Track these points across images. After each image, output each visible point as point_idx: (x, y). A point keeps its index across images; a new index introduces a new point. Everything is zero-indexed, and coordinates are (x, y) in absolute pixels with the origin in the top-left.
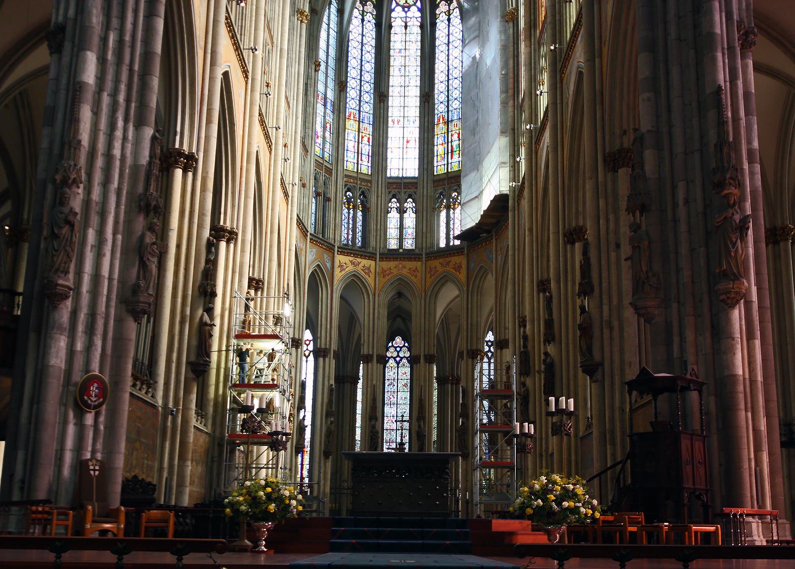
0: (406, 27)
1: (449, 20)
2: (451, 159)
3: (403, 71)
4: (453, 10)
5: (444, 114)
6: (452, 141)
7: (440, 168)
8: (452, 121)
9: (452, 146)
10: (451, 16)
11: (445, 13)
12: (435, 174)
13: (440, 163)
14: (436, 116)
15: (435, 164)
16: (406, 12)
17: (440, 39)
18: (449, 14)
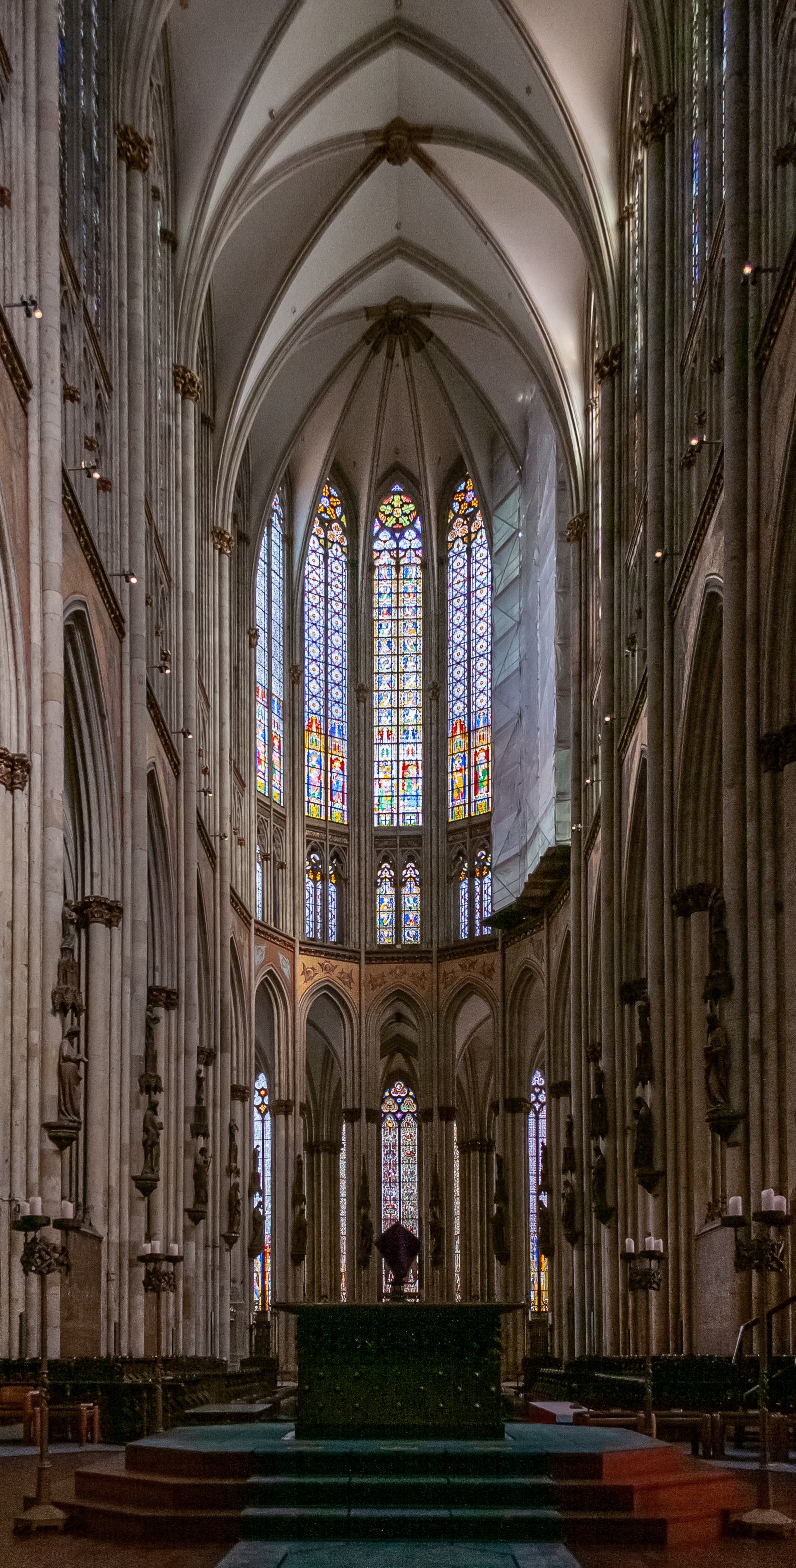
0: (398, 567)
1: (469, 551)
2: (476, 794)
3: (394, 647)
4: (477, 533)
5: (462, 719)
6: (476, 764)
7: (457, 812)
8: (476, 730)
9: (477, 774)
10: (474, 545)
11: (463, 538)
12: (451, 820)
13: (458, 803)
14: (450, 723)
15: (451, 805)
16: (398, 541)
17: (456, 587)
18: (469, 539)
